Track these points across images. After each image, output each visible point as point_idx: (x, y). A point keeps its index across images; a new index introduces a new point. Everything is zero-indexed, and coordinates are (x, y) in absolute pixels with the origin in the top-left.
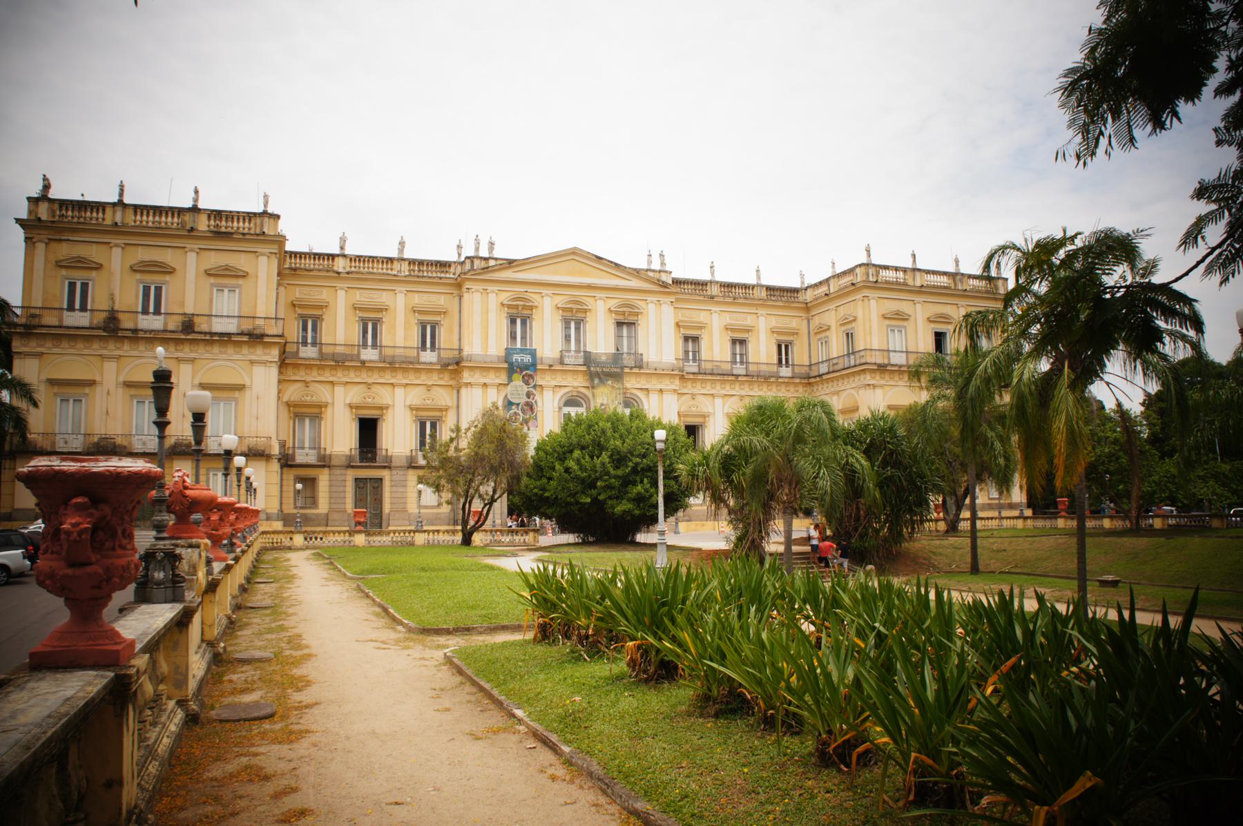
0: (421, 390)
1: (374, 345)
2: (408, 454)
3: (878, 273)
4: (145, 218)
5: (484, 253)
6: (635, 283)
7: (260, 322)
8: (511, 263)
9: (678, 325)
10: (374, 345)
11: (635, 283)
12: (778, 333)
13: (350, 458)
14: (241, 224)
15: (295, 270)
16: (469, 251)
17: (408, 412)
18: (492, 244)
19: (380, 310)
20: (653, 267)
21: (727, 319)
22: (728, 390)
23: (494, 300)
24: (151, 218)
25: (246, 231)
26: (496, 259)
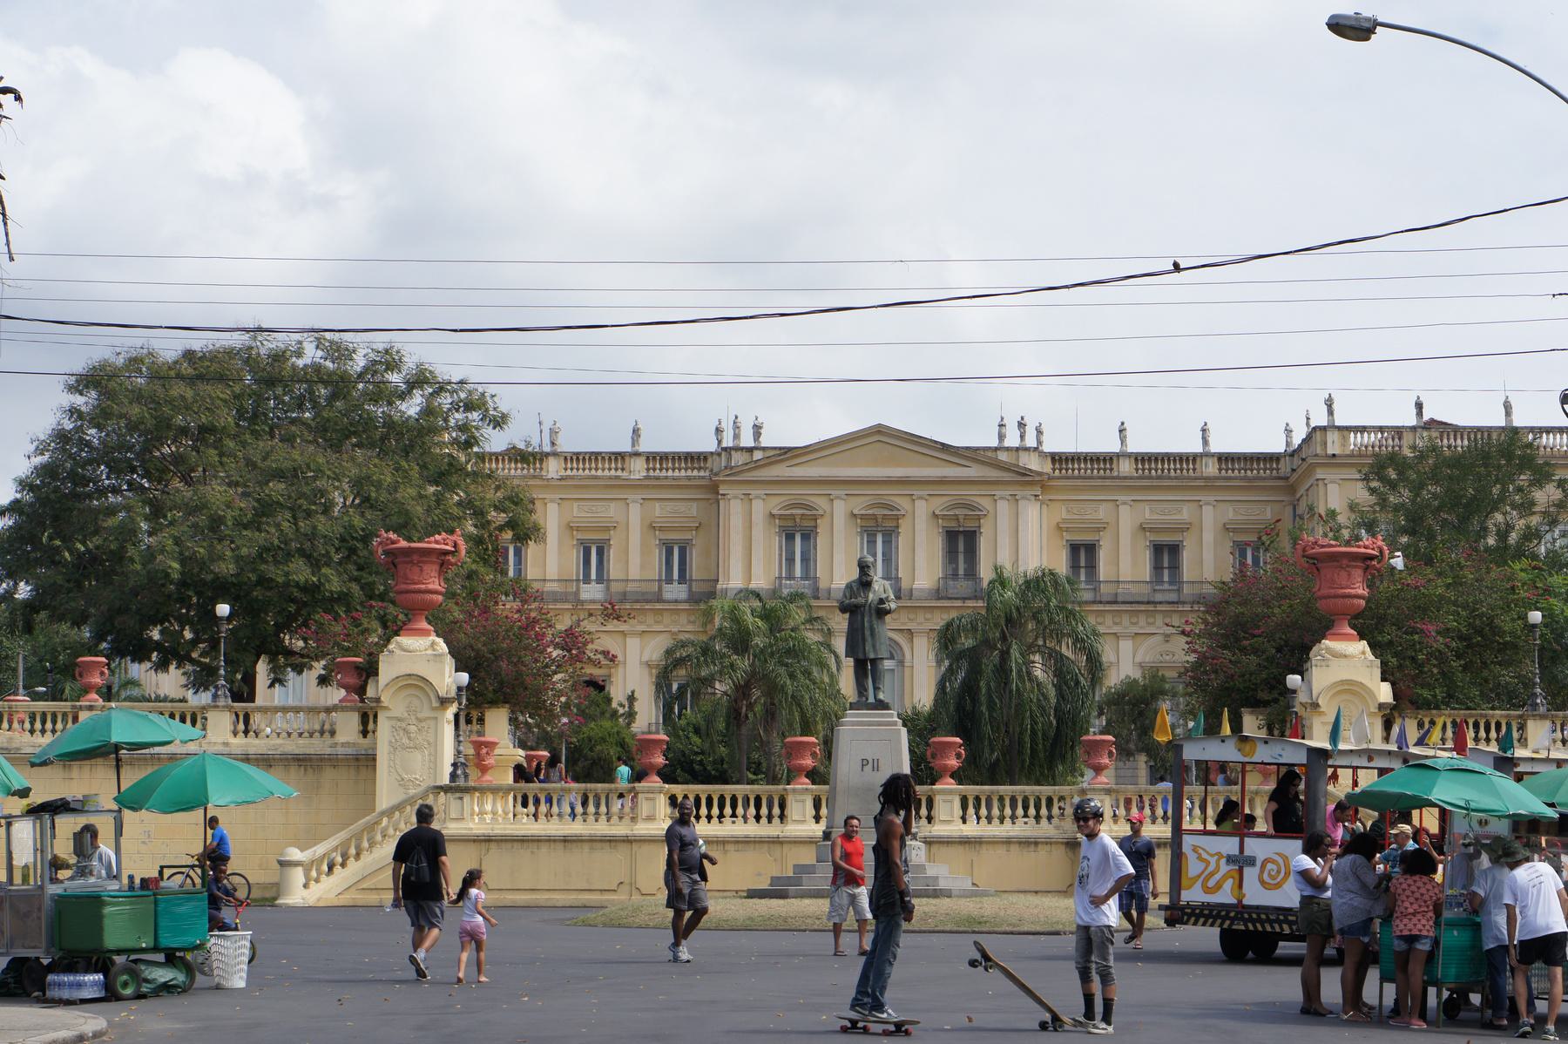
1: (600, 580)
3: (1345, 439)
5: (747, 440)
6: (974, 472)
8: (786, 454)
9: (1059, 528)
10: (600, 580)
11: (974, 472)
12: (1234, 530)
16: (728, 441)
17: (646, 671)
18: (757, 430)
19: (607, 529)
20: (1007, 443)
21: (1147, 514)
22: (1143, 625)
23: (759, 509)
26: (764, 449)
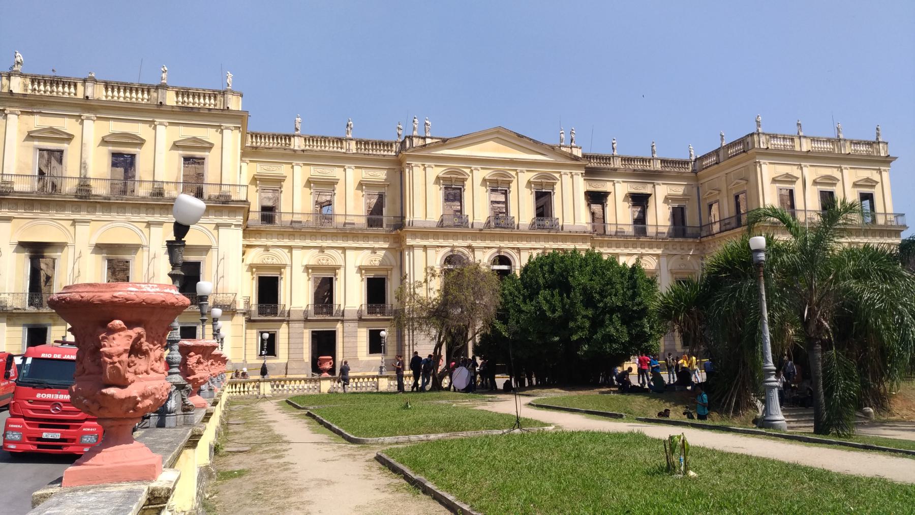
2: (358, 308)
4: (116, 93)
7: (224, 188)
13: (306, 312)
14: (207, 101)
15: (256, 148)
24: (122, 94)
25: (212, 107)
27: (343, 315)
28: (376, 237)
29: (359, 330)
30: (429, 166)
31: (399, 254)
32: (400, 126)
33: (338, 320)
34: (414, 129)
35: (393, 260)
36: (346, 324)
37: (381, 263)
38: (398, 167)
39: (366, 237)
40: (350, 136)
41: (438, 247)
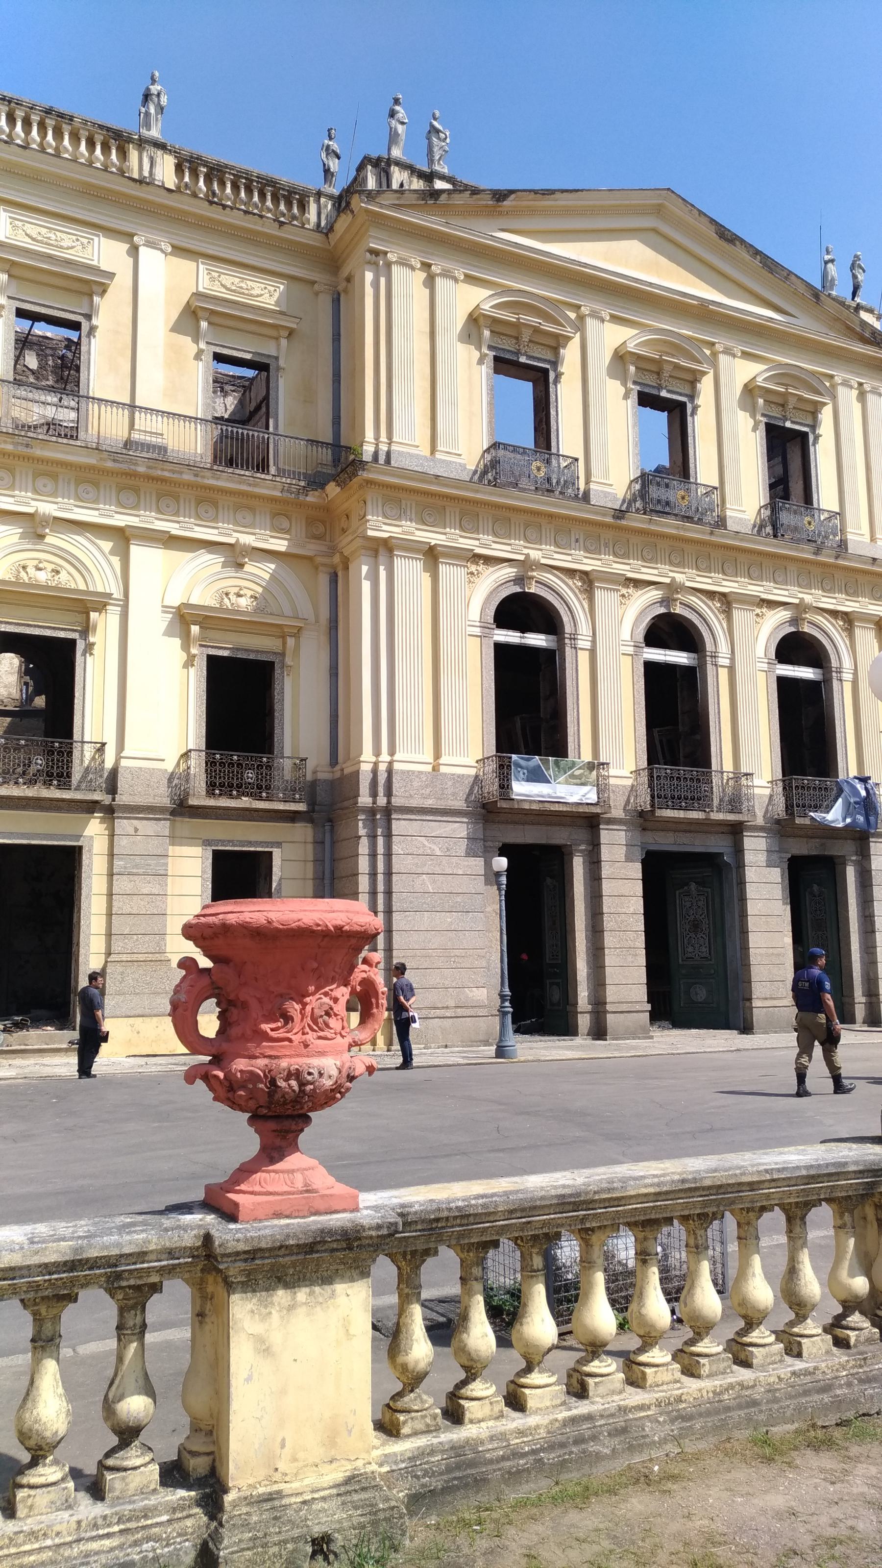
0: (211, 561)
2: (169, 766)
27: (112, 788)
28: (244, 507)
29: (173, 850)
30: (447, 274)
31: (323, 580)
32: (334, 145)
33: (91, 807)
34: (393, 138)
35: (305, 601)
36: (123, 825)
37: (262, 602)
38: (330, 276)
39: (206, 501)
40: (154, 133)
41: (477, 558)
